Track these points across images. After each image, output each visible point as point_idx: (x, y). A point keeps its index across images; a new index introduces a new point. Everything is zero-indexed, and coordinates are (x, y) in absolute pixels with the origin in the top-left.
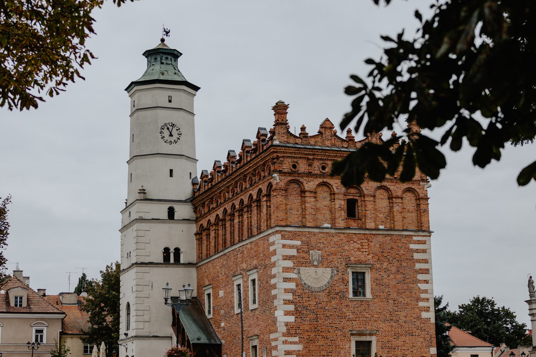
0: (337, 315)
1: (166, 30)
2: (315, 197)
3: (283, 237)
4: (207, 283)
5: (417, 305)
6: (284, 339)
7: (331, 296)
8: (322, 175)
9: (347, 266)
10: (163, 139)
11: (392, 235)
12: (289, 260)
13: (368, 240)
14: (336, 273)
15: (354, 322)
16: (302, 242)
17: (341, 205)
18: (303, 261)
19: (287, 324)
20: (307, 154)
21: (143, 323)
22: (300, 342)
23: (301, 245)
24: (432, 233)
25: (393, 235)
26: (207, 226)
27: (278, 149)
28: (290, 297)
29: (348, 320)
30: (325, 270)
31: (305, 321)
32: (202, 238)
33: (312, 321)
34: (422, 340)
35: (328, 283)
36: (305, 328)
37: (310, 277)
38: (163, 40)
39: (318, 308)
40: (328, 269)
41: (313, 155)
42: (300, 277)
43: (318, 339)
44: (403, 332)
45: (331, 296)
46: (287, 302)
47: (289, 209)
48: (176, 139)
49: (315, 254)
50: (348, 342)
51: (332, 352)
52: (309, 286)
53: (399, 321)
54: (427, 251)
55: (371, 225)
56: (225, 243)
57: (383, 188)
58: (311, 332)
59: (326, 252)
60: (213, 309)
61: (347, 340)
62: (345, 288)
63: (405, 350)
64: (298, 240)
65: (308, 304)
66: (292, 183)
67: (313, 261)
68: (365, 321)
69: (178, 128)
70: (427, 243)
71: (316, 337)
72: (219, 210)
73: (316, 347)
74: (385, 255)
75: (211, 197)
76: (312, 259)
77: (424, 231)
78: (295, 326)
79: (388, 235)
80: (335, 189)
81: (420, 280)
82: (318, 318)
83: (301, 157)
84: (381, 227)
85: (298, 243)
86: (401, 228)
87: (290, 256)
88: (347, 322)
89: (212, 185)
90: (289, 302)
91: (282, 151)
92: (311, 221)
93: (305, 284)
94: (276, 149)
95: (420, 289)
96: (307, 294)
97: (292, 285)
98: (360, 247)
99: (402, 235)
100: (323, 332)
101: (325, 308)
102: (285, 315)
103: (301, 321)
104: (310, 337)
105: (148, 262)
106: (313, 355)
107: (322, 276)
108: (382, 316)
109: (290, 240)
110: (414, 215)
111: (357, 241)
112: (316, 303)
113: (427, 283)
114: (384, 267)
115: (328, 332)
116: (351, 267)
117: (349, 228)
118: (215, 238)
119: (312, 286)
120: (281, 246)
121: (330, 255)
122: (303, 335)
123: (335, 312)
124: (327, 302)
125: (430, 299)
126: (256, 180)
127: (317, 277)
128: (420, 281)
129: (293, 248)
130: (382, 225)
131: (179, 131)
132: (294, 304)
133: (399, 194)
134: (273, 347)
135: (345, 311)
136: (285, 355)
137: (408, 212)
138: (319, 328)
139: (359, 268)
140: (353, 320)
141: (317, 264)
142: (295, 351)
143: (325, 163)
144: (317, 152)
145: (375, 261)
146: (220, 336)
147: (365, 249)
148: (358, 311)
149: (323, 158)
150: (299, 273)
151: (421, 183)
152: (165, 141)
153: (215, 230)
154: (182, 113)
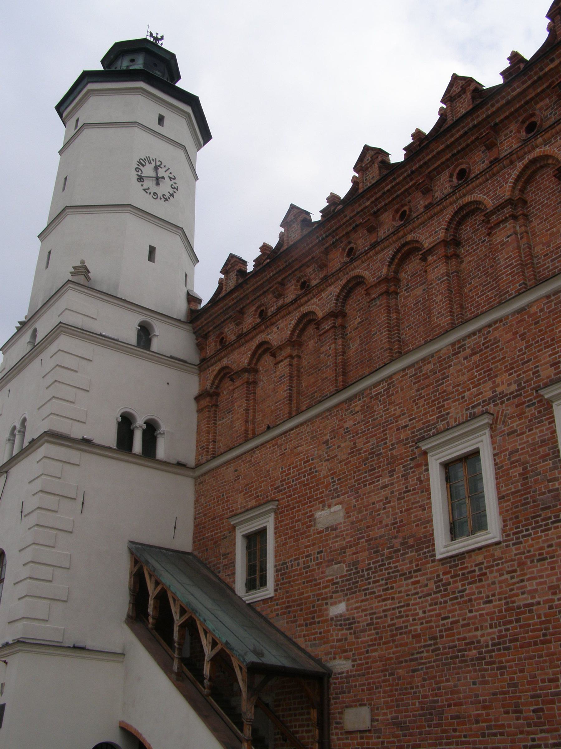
4: (253, 503)
10: (141, 183)
21: (48, 602)
26: (250, 363)
32: (217, 406)
48: (167, 195)
56: (344, 374)
60: (277, 571)
69: (171, 176)
72: (315, 300)
75: (279, 279)
105: (80, 437)
118: (291, 377)
131: (174, 181)
146: (319, 651)
152: (145, 187)
153: (291, 357)
154: (181, 153)
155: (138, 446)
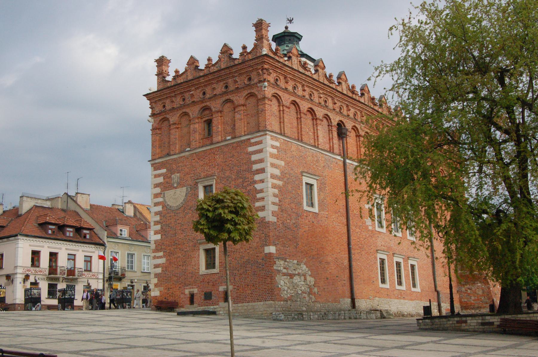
1: (289, 19)
6: (153, 254)
7: (186, 211)
11: (233, 143)
18: (167, 185)
22: (164, 256)
25: (234, 143)
28: (158, 218)
34: (258, 240)
35: (184, 200)
38: (286, 28)
40: (184, 188)
41: (174, 92)
42: (165, 200)
45: (186, 211)
46: (156, 223)
49: (176, 177)
66: (164, 121)
67: (174, 184)
70: (263, 142)
79: (229, 144)
85: (164, 171)
93: (168, 205)
95: (256, 189)
97: (159, 208)
99: (241, 141)
102: (155, 234)
113: (263, 182)
116: (200, 182)
120: (153, 176)
128: (256, 182)
133: (242, 101)
136: (154, 268)
142: (160, 264)
144: (175, 88)
150: (164, 196)
151: (258, 85)
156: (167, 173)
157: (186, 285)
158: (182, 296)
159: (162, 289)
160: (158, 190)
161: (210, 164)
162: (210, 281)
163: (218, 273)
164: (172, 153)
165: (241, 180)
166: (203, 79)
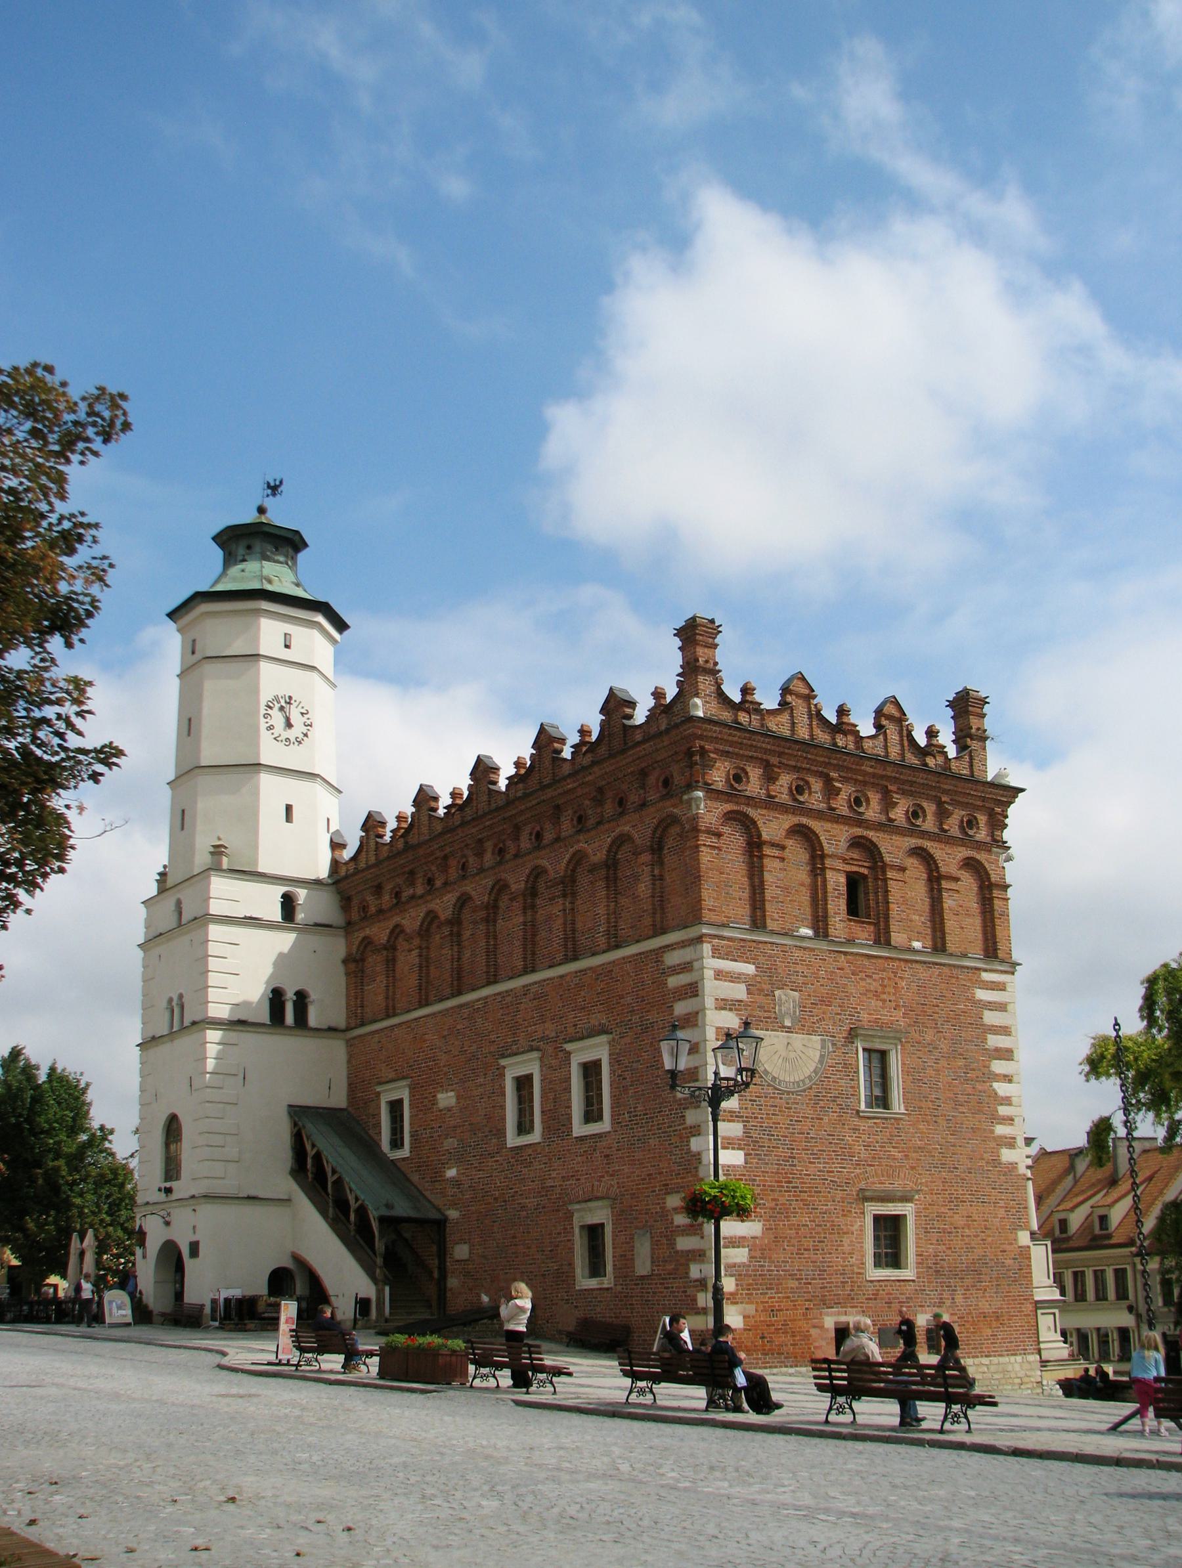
0: (834, 1151)
2: (782, 859)
3: (717, 953)
5: (992, 1132)
8: (800, 809)
9: (852, 1035)
12: (731, 1010)
13: (895, 973)
14: (831, 1050)
15: (869, 1169)
16: (757, 967)
17: (837, 884)
19: (728, 1171)
20: (766, 751)
23: (756, 976)
24: (1017, 967)
27: (706, 730)
29: (857, 1165)
30: (810, 1040)
31: (767, 1164)
33: (781, 1165)
34: (1001, 1213)
35: (815, 1071)
36: (766, 1181)
37: (776, 1057)
39: (794, 1133)
41: (780, 754)
43: (794, 1208)
44: (965, 1194)
47: (726, 886)
49: (787, 999)
50: (859, 1217)
51: (823, 1242)
52: (774, 1078)
53: (957, 1168)
54: (1009, 1007)
55: (897, 938)
57: (918, 854)
58: (781, 1191)
59: (809, 995)
61: (856, 1213)
62: (852, 1087)
63: (969, 1236)
64: (749, 963)
65: (774, 1123)
67: (783, 1017)
68: (891, 1166)
71: (791, 1205)
73: (791, 1229)
74: (930, 1012)
76: (780, 1010)
77: (1003, 961)
78: (744, 1175)
80: (825, 845)
81: (997, 1075)
82: (794, 1158)
83: (751, 757)
84: (917, 945)
85: (750, 969)
86: (958, 951)
87: (732, 1001)
88: (855, 1169)
89: (406, 843)
90: (732, 1116)
91: (714, 735)
92: (776, 916)
94: (700, 728)
95: (996, 1094)
96: (771, 1098)
98: (880, 989)
100: (806, 1192)
101: (808, 1134)
103: (757, 1163)
104: (777, 1205)
106: (784, 1249)
107: (801, 1054)
108: (925, 1156)
109: (731, 960)
110: (977, 921)
111: (873, 973)
112: (791, 1121)
113: (1010, 1081)
114: (928, 1038)
115: (816, 1192)
117: (850, 941)
119: (781, 1079)
120: (711, 973)
121: (816, 1004)
122: (762, 1199)
123: (831, 1143)
124: (812, 1118)
125: (1016, 1119)
126: (603, 815)
127: (792, 1055)
129: (739, 982)
130: (918, 941)
132: (743, 1121)
134: (679, 1227)
135: (851, 1142)
137: (969, 915)
138: (796, 1183)
139: (878, 1040)
140: (868, 1165)
141: (790, 1025)
142: (744, 1237)
143: (803, 779)
145: (909, 1025)
147: (889, 993)
148: (877, 1142)
149: (799, 764)
155: (289, 1018)
156: (758, 979)
157: (825, 1303)
158: (813, 1332)
159: (751, 1309)
160: (732, 1021)
161: (884, 997)
162: (894, 1298)
163: (913, 1281)
164: (770, 924)
165: (961, 1063)
166: (871, 767)
